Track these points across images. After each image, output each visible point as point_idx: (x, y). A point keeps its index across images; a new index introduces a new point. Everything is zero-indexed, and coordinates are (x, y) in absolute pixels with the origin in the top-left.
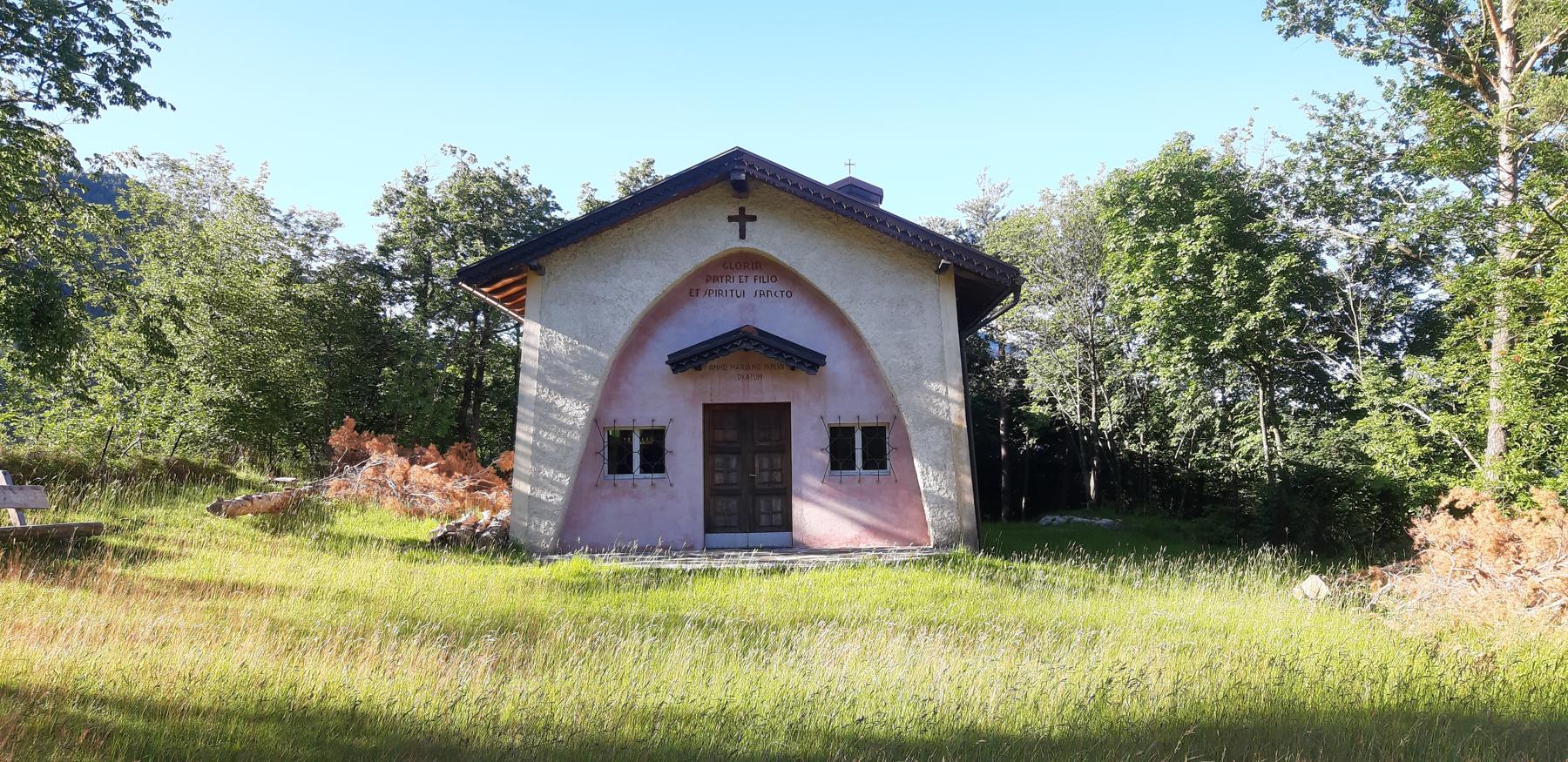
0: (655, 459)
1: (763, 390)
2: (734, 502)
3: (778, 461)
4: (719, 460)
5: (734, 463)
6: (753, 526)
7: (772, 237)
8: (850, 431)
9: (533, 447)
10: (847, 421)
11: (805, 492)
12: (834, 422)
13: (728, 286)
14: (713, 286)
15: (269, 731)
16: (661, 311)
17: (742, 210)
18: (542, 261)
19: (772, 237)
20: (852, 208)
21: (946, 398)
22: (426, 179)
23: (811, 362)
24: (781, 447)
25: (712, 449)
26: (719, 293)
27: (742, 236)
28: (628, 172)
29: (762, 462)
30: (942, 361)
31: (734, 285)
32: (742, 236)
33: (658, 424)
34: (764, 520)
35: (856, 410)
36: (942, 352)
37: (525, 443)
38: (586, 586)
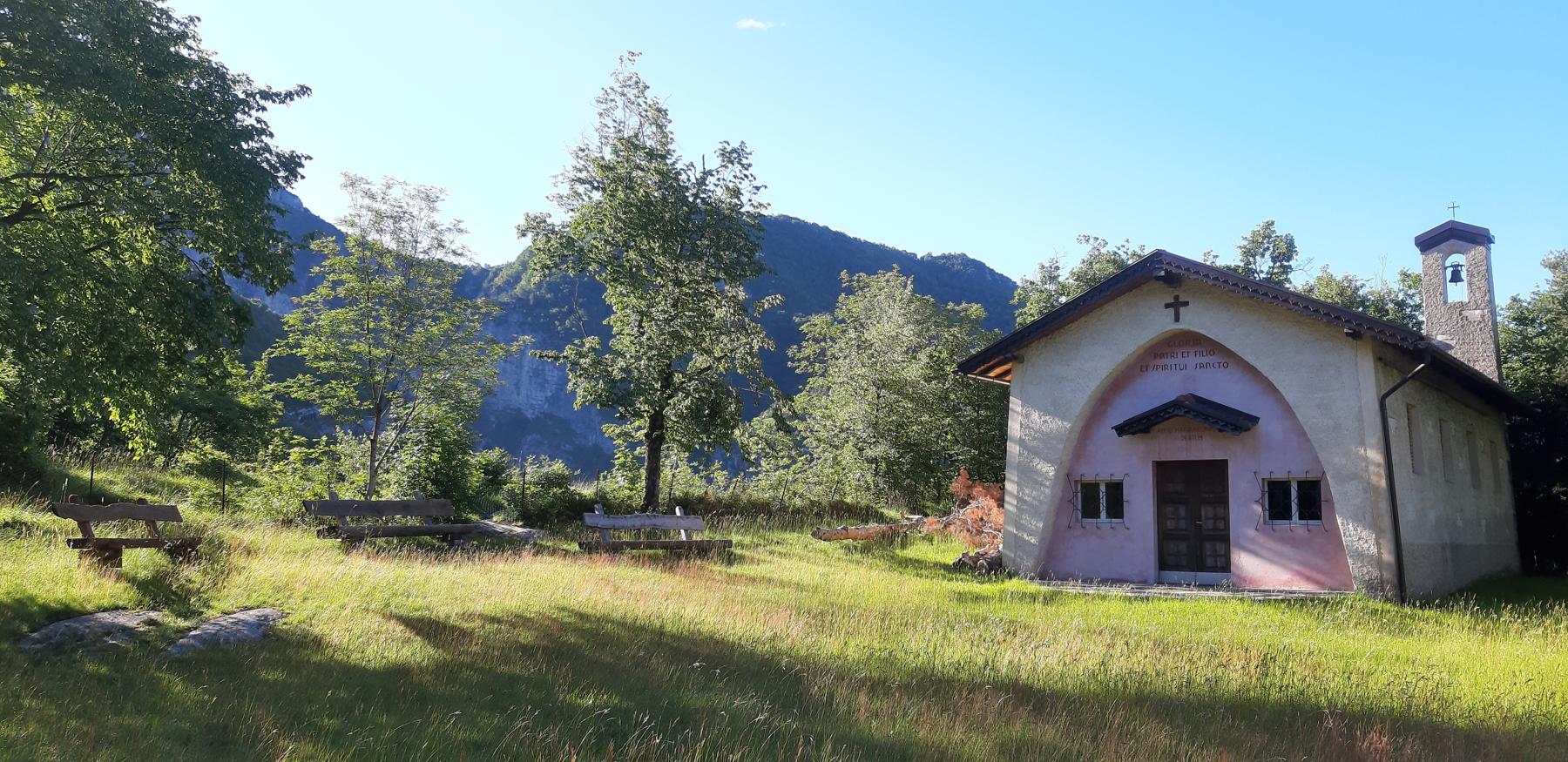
0: (1116, 508)
1: (1204, 449)
2: (1183, 546)
3: (1220, 510)
4: (1170, 509)
5: (1182, 511)
6: (1200, 566)
7: (1200, 318)
8: (1096, 486)
9: (1017, 498)
10: (1279, 476)
11: (1242, 542)
12: (1267, 476)
13: (1172, 361)
14: (1160, 362)
15: (623, 633)
16: (1117, 384)
17: (1177, 297)
18: (1022, 352)
19: (1200, 318)
20: (1256, 291)
21: (1366, 459)
22: (1057, 268)
23: (1237, 423)
24: (1221, 499)
25: (1164, 499)
26: (1165, 367)
27: (1177, 319)
28: (1249, 236)
29: (1207, 511)
30: (1360, 420)
31: (1178, 360)
32: (1177, 319)
33: (1117, 478)
34: (1209, 562)
35: (1289, 467)
36: (1360, 411)
37: (1011, 494)
38: (961, 597)
